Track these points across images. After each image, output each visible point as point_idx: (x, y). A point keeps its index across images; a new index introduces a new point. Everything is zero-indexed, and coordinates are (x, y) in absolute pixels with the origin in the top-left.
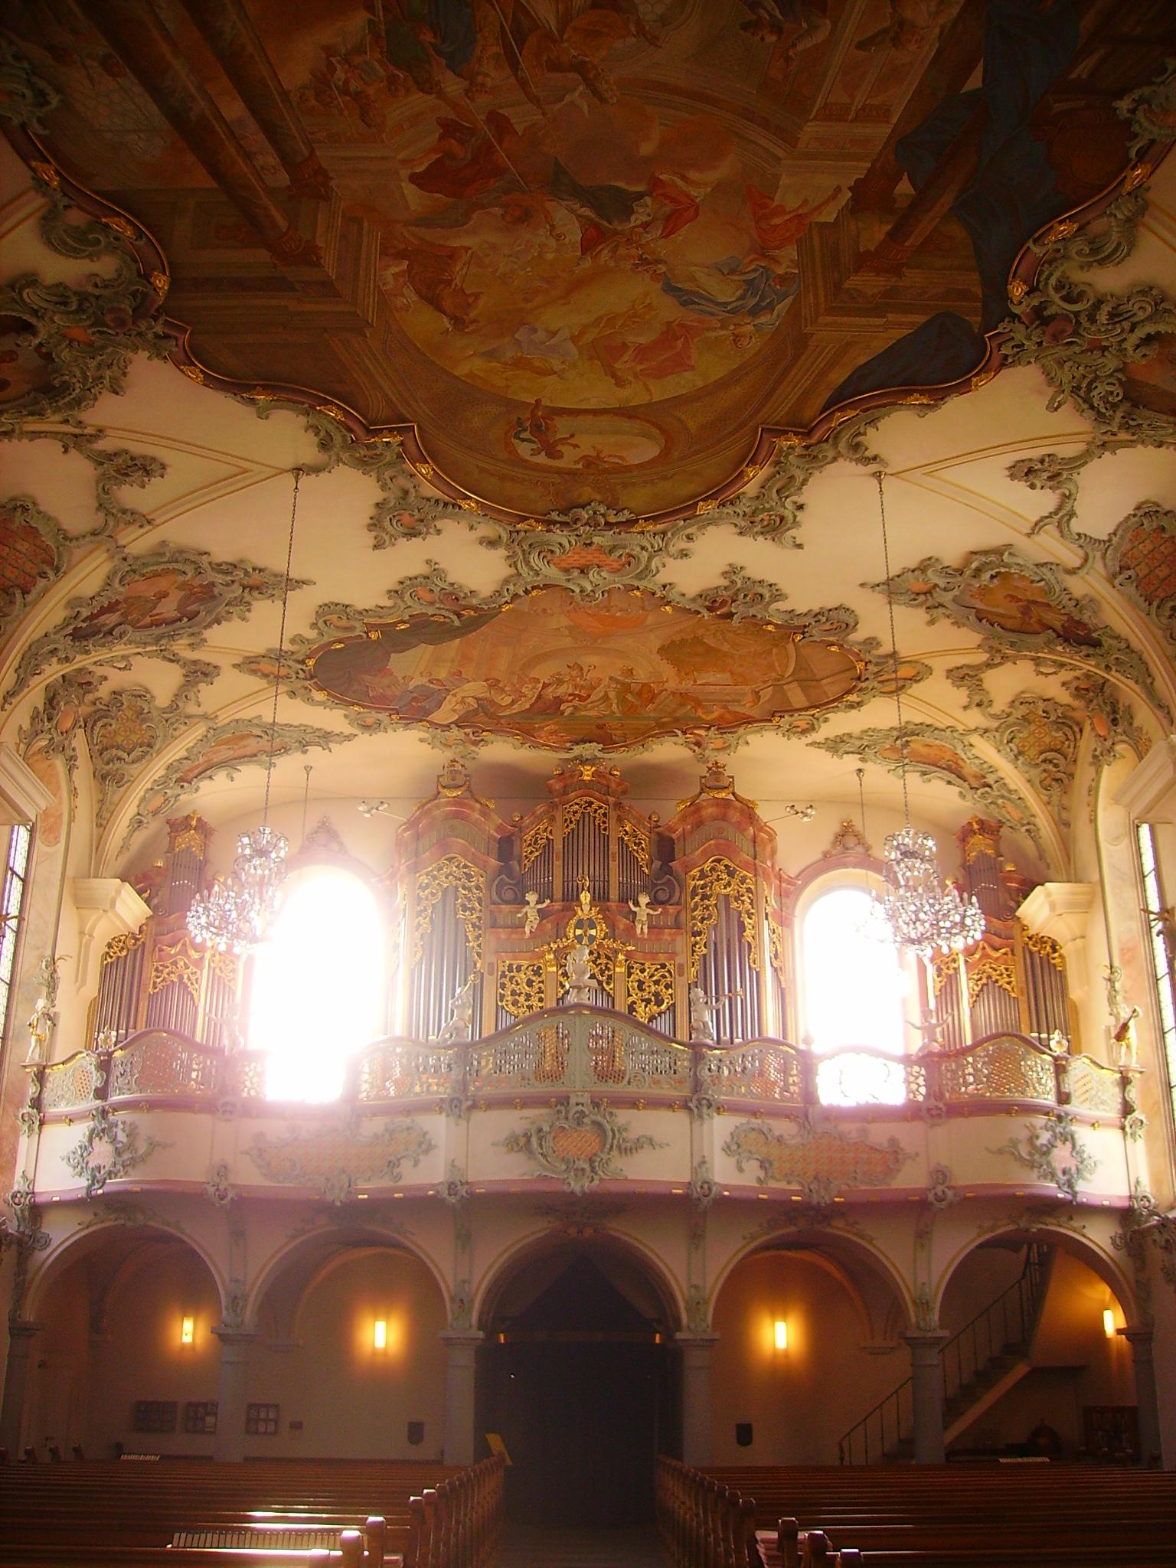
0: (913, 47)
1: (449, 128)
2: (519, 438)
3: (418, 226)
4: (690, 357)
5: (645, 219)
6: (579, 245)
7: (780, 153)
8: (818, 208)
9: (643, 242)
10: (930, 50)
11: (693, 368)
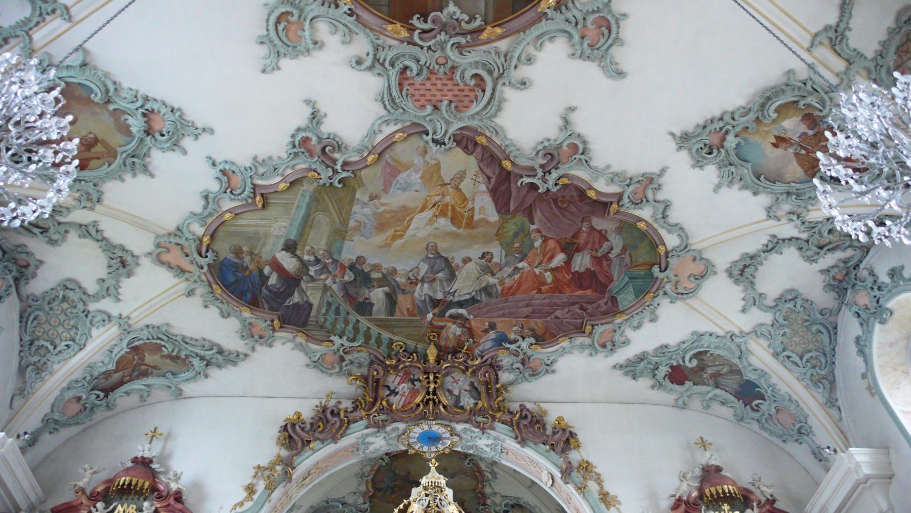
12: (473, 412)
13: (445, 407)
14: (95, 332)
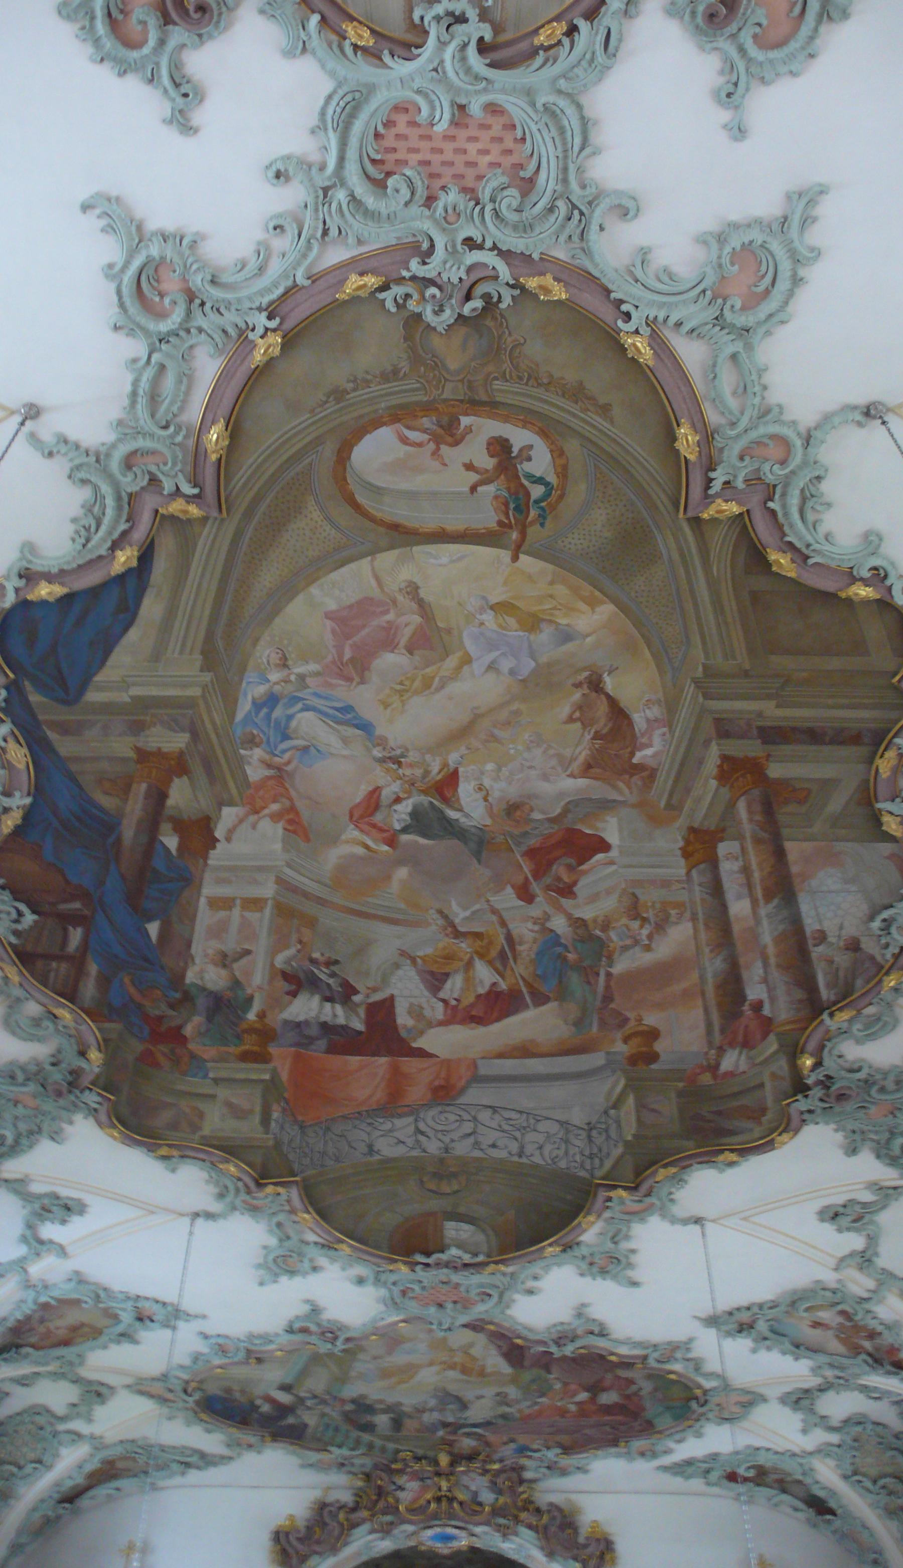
0: (210, 952)
1: (567, 891)
2: (547, 484)
3: (614, 801)
4: (333, 632)
5: (398, 807)
6: (461, 779)
7: (288, 871)
8: (241, 821)
9: (398, 782)
10: (197, 949)
11: (329, 615)
12: (497, 1511)
13: (461, 1504)
14: (64, 1451)
